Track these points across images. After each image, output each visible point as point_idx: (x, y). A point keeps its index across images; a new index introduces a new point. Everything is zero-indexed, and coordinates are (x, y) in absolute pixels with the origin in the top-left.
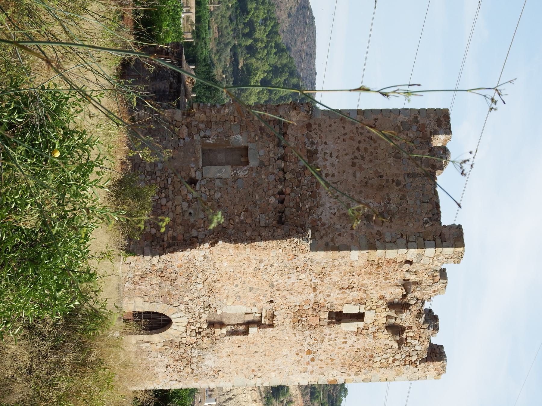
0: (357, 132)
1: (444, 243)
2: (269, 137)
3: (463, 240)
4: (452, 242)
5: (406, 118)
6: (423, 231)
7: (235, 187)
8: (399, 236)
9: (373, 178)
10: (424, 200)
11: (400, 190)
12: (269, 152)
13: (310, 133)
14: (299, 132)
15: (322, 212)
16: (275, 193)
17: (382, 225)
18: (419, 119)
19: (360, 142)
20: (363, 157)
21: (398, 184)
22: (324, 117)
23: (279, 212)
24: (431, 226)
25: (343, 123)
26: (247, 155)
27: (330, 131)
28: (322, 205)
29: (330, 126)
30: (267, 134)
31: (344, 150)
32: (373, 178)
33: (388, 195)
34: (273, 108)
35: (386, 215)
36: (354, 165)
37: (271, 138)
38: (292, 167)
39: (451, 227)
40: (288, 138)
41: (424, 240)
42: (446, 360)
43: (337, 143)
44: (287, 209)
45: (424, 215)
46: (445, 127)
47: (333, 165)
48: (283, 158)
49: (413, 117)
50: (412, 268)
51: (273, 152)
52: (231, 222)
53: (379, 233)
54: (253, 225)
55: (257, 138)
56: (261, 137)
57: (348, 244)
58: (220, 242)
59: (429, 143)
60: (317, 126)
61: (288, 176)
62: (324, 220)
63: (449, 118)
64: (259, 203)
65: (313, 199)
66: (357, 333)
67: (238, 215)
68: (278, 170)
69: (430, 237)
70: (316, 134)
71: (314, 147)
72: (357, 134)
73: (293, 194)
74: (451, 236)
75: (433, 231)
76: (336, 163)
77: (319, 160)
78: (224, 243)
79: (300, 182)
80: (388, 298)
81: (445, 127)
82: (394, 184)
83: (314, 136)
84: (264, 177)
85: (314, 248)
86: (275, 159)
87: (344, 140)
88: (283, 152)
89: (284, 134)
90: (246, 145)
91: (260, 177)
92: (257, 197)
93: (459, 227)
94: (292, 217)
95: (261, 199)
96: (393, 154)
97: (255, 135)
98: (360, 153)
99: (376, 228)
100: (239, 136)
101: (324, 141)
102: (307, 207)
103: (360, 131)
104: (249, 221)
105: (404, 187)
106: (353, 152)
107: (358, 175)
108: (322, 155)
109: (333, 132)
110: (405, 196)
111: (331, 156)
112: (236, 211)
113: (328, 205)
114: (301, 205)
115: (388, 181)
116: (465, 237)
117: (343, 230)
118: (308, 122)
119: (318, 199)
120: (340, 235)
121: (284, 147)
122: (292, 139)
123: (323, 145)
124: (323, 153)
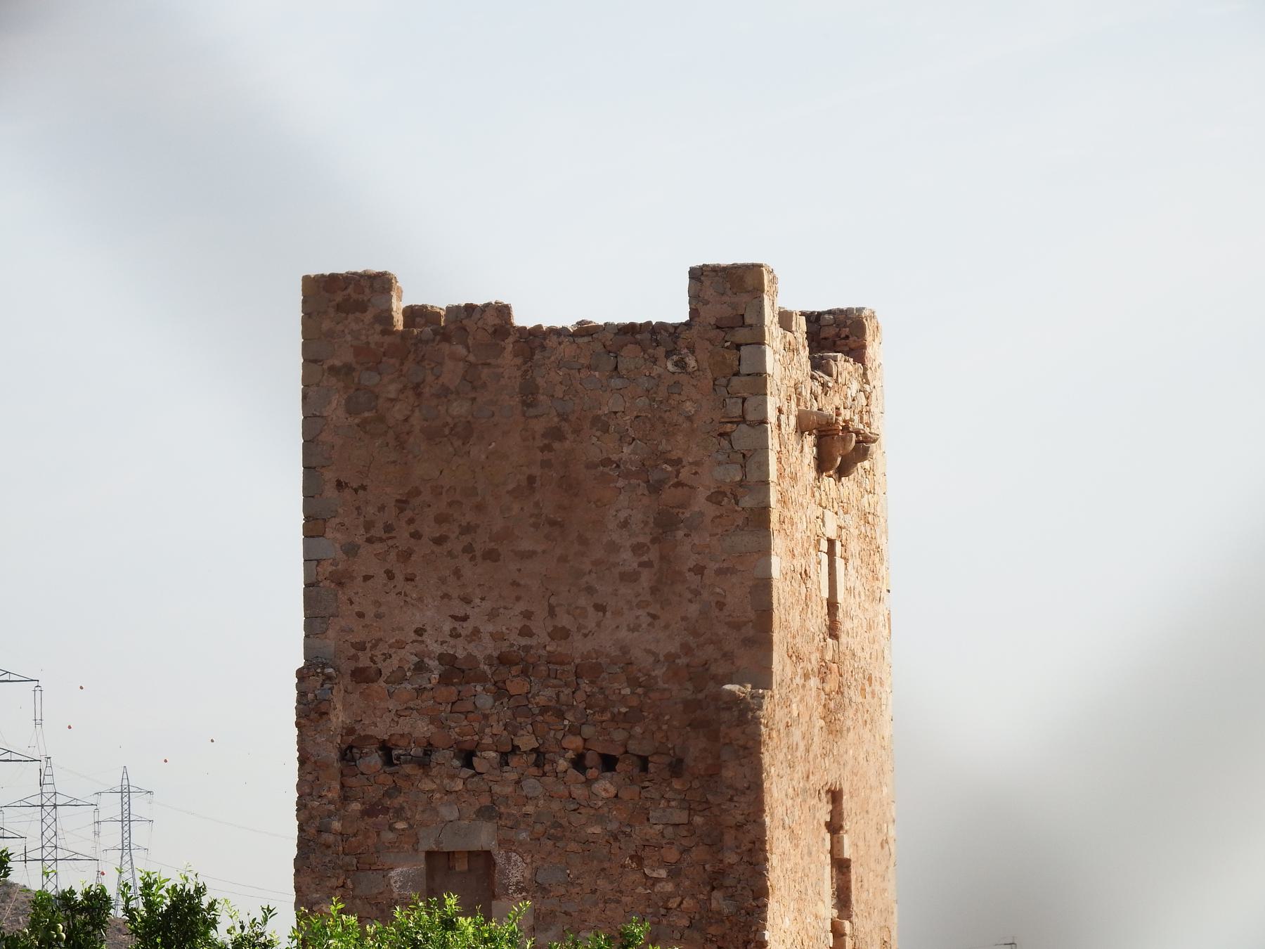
0: (381, 540)
1: (748, 321)
2: (397, 789)
3: (735, 267)
4: (744, 298)
5: (337, 400)
6: (709, 375)
7: (563, 891)
8: (725, 443)
9: (537, 504)
10: (611, 367)
11: (577, 431)
12: (448, 792)
13: (386, 673)
14: (383, 705)
15: (649, 651)
16: (582, 778)
17: (691, 487)
18: (338, 363)
19: (416, 535)
20: (467, 529)
21: (556, 434)
22: (331, 633)
23: (644, 769)
24: (693, 352)
25: (352, 578)
26: (450, 855)
27: (378, 616)
28: (624, 650)
29: (361, 615)
30: (387, 794)
31: (443, 580)
32: (537, 504)
33: (591, 466)
34: (310, 778)
35: (655, 476)
36: (492, 556)
37: (400, 783)
38: (498, 728)
39: (695, 298)
40: (402, 735)
41: (737, 374)
42: (860, 310)
43: (420, 599)
44: (633, 747)
45: (657, 370)
46: (367, 291)
47: (493, 615)
48: (467, 758)
49: (333, 380)
50: (785, 409)
51: (446, 781)
52: (673, 904)
53: (716, 497)
54: (685, 842)
55: (401, 825)
56: (399, 813)
57: (751, 583)
58: (768, 935)
59: (421, 341)
60: (360, 654)
61: (526, 741)
62: (673, 647)
63: (333, 278)
64: (613, 826)
65: (604, 675)
66: (846, 560)
67: (653, 885)
68: (506, 768)
69: (730, 356)
70: (387, 656)
71: (433, 664)
72: (390, 542)
73: (588, 731)
74: (725, 298)
75: (710, 347)
76: (487, 605)
77: (476, 653)
78: (768, 925)
79: (544, 710)
80: (813, 474)
81: (367, 291)
82: (556, 445)
83: (395, 662)
84: (529, 809)
85: (762, 677)
86: (473, 776)
87: (410, 579)
88: (449, 753)
89: (386, 749)
90: (423, 855)
91: (531, 820)
92: (597, 830)
93: (698, 275)
94: (659, 735)
95: (600, 820)
96: (458, 443)
97: (392, 829)
98: (453, 536)
99: (700, 503)
100: (392, 873)
101: (413, 636)
102: (627, 691)
103: (378, 531)
104: (672, 855)
105: (566, 420)
106: (450, 553)
107: (526, 545)
108: (460, 642)
109: (383, 609)
110: (596, 420)
111: (465, 618)
112: (640, 890)
113: (623, 634)
114: (623, 710)
115: (546, 464)
116: (725, 260)
117: (705, 595)
118: (347, 679)
119: (603, 660)
120: (721, 605)
121: (429, 749)
122: (404, 726)
123: (424, 638)
124: (452, 641)
